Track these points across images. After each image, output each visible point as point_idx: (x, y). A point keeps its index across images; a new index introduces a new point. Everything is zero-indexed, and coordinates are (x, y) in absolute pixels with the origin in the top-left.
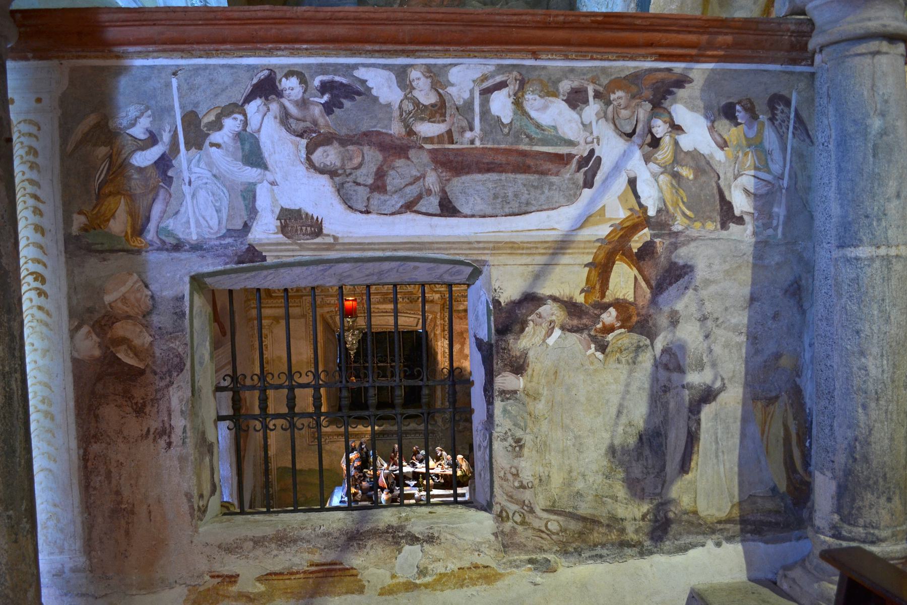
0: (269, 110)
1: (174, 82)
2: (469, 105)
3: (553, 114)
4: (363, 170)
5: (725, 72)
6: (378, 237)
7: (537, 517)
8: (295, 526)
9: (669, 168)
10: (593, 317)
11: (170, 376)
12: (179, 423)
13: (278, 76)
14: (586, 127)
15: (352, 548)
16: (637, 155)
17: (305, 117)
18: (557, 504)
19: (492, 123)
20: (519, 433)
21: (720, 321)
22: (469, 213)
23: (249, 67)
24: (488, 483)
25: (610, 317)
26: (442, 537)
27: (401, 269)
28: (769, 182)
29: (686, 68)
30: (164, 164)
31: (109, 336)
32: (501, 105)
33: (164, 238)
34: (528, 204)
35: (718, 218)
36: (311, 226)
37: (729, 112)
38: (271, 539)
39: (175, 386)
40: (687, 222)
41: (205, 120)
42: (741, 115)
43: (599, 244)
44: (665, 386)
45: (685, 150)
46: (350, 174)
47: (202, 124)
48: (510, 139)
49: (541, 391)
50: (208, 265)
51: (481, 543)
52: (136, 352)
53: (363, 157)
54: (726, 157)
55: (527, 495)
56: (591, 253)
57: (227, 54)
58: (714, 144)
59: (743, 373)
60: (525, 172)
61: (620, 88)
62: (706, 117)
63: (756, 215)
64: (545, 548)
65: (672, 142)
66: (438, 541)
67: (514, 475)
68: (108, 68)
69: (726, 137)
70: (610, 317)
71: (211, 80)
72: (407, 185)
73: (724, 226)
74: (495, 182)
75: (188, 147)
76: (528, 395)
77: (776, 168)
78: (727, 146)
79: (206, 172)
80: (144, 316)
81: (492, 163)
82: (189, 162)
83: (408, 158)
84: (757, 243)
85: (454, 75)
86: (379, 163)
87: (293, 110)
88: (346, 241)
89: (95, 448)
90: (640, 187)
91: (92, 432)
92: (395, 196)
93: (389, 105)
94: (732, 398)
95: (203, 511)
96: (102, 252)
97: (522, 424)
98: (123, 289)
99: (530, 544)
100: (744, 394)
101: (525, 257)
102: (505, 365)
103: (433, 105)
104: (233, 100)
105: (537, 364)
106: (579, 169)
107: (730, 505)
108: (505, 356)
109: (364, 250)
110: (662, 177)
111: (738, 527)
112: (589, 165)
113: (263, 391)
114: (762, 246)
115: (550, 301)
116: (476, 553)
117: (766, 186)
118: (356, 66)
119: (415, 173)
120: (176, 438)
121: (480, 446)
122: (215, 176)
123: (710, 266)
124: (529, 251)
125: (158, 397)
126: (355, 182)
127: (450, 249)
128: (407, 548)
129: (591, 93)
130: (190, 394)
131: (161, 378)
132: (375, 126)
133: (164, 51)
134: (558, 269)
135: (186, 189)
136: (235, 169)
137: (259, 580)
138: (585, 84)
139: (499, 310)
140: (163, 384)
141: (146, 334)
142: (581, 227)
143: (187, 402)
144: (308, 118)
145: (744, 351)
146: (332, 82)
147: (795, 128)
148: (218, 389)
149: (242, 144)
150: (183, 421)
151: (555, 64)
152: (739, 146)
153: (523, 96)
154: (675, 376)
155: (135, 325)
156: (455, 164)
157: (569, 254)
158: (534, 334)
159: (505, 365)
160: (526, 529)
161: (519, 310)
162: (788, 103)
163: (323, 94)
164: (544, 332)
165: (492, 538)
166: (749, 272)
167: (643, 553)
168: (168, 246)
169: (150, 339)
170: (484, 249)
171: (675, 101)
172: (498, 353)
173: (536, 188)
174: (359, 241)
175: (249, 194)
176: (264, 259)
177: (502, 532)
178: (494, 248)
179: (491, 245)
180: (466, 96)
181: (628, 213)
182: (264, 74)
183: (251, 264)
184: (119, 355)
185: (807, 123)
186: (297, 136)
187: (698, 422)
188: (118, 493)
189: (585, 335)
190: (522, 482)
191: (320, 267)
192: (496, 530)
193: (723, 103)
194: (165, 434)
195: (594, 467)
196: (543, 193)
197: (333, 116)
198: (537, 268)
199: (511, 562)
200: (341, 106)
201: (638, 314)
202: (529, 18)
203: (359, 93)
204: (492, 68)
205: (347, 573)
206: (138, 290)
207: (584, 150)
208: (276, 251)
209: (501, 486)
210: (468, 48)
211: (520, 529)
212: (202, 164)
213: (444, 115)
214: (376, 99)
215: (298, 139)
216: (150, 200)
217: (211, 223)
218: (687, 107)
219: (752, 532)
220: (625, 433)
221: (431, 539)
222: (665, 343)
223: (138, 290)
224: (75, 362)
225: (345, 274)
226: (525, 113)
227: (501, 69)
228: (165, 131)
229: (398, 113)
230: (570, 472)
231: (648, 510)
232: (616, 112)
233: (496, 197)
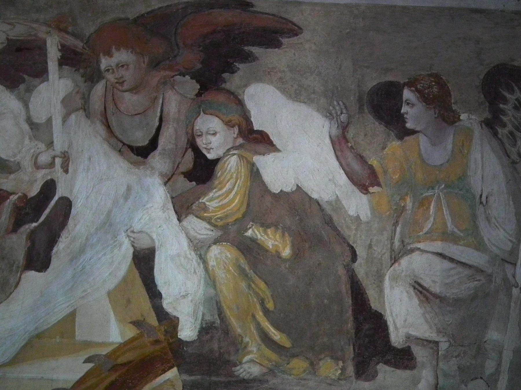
9: (233, 229)
14: (39, 130)
28: (479, 270)
35: (350, 351)
37: (384, 105)
40: (274, 356)
42: (413, 111)
45: (275, 188)
54: (373, 209)
58: (342, 178)
61: (121, 44)
62: (329, 116)
63: (444, 346)
65: (244, 171)
69: (374, 162)
73: (363, 369)
106: (17, 223)
110: (215, 251)
117: (471, 278)
129: (53, 54)
138: (42, 32)
181: (131, 332)
193: (371, 83)
207: (32, 182)
218: (284, 91)
232: (111, 97)
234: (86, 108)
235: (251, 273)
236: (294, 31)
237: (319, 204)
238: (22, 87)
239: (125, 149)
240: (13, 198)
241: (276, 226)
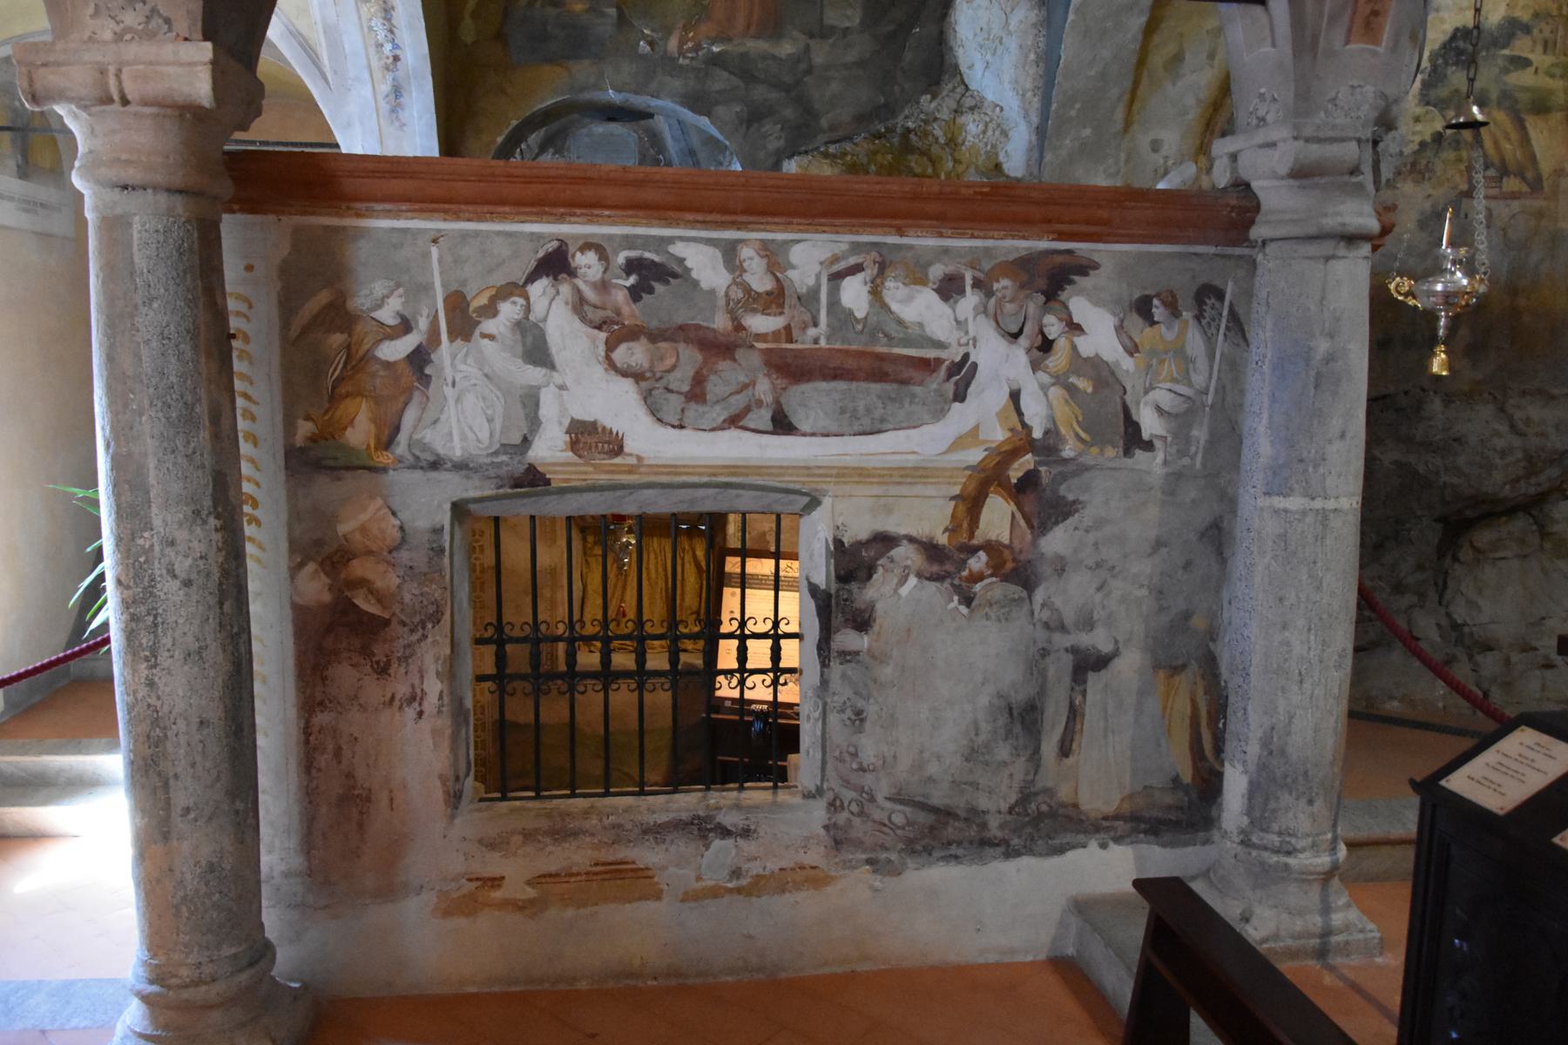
1: (434, 251)
2: (814, 292)
3: (919, 308)
4: (677, 374)
13: (571, 249)
14: (960, 324)
20: (860, 704)
23: (536, 238)
30: (419, 359)
31: (342, 576)
34: (883, 420)
36: (609, 443)
37: (1143, 308)
39: (430, 640)
41: (475, 304)
42: (1158, 312)
52: (380, 599)
55: (868, 780)
57: (504, 217)
58: (1121, 349)
61: (1006, 275)
62: (1114, 314)
65: (1068, 346)
68: (344, 228)
69: (1137, 340)
70: (978, 562)
71: (483, 252)
73: (1127, 452)
75: (453, 334)
76: (874, 657)
77: (1199, 379)
78: (1137, 350)
83: (735, 360)
85: (797, 254)
88: (652, 462)
89: (322, 718)
91: (319, 699)
92: (718, 408)
93: (712, 292)
94: (1130, 665)
96: (333, 469)
98: (363, 517)
103: (768, 293)
104: (512, 279)
106: (949, 376)
109: (677, 474)
112: (962, 375)
114: (1176, 479)
115: (905, 542)
118: (671, 240)
119: (743, 379)
122: (486, 376)
123: (1107, 503)
128: (717, 844)
129: (969, 281)
130: (448, 651)
131: (412, 631)
133: (422, 211)
135: (448, 391)
137: (528, 883)
147: (1227, 328)
148: (478, 641)
149: (523, 336)
151: (924, 242)
156: (793, 368)
162: (1220, 295)
163: (628, 274)
164: (895, 581)
165: (823, 832)
167: (1011, 853)
168: (424, 464)
169: (398, 581)
175: (531, 401)
176: (548, 482)
178: (838, 476)
179: (834, 472)
180: (811, 281)
181: (1008, 434)
182: (552, 246)
185: (1243, 319)
187: (1084, 694)
188: (350, 775)
189: (947, 584)
191: (618, 493)
193: (1137, 295)
197: (640, 304)
199: (844, 862)
200: (651, 291)
201: (1014, 560)
202: (895, 188)
203: (675, 276)
204: (845, 247)
205: (640, 874)
210: (817, 220)
211: (857, 821)
212: (470, 360)
213: (781, 306)
214: (696, 284)
216: (400, 405)
219: (1145, 832)
221: (746, 833)
224: (295, 607)
226: (885, 307)
233: (843, 411)
236: (1096, 266)
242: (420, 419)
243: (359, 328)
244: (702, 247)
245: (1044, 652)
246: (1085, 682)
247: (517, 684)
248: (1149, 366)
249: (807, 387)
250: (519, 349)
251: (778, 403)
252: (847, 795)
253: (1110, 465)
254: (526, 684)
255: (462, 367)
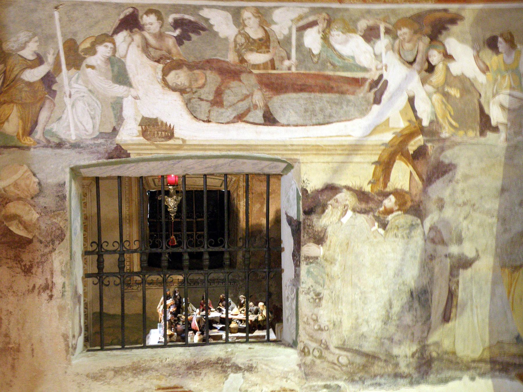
0: (133, 40)
1: (56, 14)
3: (353, 47)
4: (206, 89)
5: (491, 11)
6: (217, 140)
7: (331, 353)
8: (146, 358)
9: (440, 89)
10: (376, 202)
11: (53, 244)
12: (59, 280)
13: (140, 14)
14: (377, 57)
15: (190, 376)
16: (416, 78)
17: (161, 46)
18: (346, 343)
19: (305, 54)
20: (319, 289)
21: (477, 206)
22: (286, 123)
24: (295, 326)
25: (390, 202)
26: (259, 367)
27: (232, 164)
29: (459, 9)
30: (49, 80)
32: (312, 39)
33: (49, 138)
34: (330, 116)
35: (478, 128)
36: (165, 131)
37: (492, 44)
38: (128, 369)
39: (57, 251)
41: (83, 47)
42: (502, 45)
43: (383, 147)
44: (431, 255)
46: (196, 92)
47: (80, 50)
48: (318, 66)
49: (336, 257)
50: (84, 159)
51: (289, 372)
53: (206, 79)
54: (488, 80)
55: (324, 336)
56: (377, 154)
58: (477, 69)
59: (494, 247)
60: (329, 92)
61: (405, 26)
62: (473, 48)
63: (509, 125)
64: (337, 376)
65: (444, 68)
66: (256, 370)
67: (314, 320)
70: (390, 202)
71: (87, 14)
72: (239, 101)
73: (482, 133)
74: (306, 99)
75: (69, 66)
76: (326, 260)
79: (84, 87)
80: (32, 198)
81: (304, 85)
82: (70, 79)
83: (240, 81)
84: (508, 148)
86: (218, 84)
87: (152, 41)
88: (191, 143)
90: (418, 104)
92: (230, 110)
93: (226, 39)
94: (485, 266)
95: (74, 348)
97: (321, 282)
98: (15, 177)
99: (326, 374)
100: (495, 263)
101: (326, 156)
102: (310, 238)
103: (260, 40)
104: (104, 31)
105: (334, 237)
106: (371, 89)
107: (482, 349)
108: (310, 231)
109: (205, 150)
111: (489, 366)
112: (378, 87)
113: (122, 254)
116: (285, 380)
119: (245, 92)
120: (56, 292)
121: (288, 298)
122: (90, 91)
123: (470, 164)
124: (330, 153)
125: (43, 260)
126: (199, 98)
127: (271, 150)
128: (232, 376)
129: (382, 30)
130: (69, 258)
131: (46, 246)
132: (215, 55)
134: (351, 166)
135: (67, 100)
136: (106, 86)
138: (378, 22)
139: (307, 196)
140: (47, 250)
141: (34, 212)
142: (371, 134)
143: (67, 264)
144: (164, 48)
145: (495, 229)
146: (182, 19)
149: (112, 67)
150: (63, 279)
152: (499, 71)
153: (329, 32)
154: (440, 248)
155: (25, 205)
156: (275, 84)
157: (360, 154)
158: (332, 214)
159: (310, 238)
160: (322, 362)
161: (321, 196)
164: (339, 213)
165: (297, 368)
166: (501, 169)
168: (52, 144)
169: (37, 216)
170: (296, 150)
171: (449, 35)
172: (304, 228)
173: (337, 104)
174: (201, 143)
175: (117, 106)
176: (128, 155)
177: (304, 363)
178: (304, 150)
179: (301, 147)
180: (286, 32)
181: (407, 124)
183: (119, 160)
184: (11, 228)
186: (156, 61)
187: (457, 283)
188: (7, 335)
189: (371, 215)
190: (320, 326)
191: (171, 162)
192: (300, 362)
194: (48, 288)
195: (376, 316)
196: (342, 108)
197: (183, 47)
198: (335, 165)
199: (311, 387)
200: (189, 39)
203: (204, 29)
204: (306, 10)
206: (28, 178)
208: (138, 149)
209: (304, 329)
211: (318, 361)
212: (80, 81)
213: (268, 47)
214: (216, 34)
215: (156, 64)
216: (38, 109)
217: (87, 127)
218: (459, 40)
220: (400, 290)
221: (250, 369)
222: (432, 223)
223: (28, 178)
225: (189, 167)
226: (330, 46)
227: (314, 11)
228: (49, 54)
229: (233, 45)
230: (357, 318)
231: (417, 350)
232: (401, 45)
233: (306, 111)
234: (393, 49)
235: (446, 103)
237: (470, 80)
238: (372, 43)
239: (406, 63)
240: (369, 81)
241: (455, 87)
242: (50, 118)
243: (11, 61)
244: (220, 11)
245: (432, 258)
246: (458, 275)
247: (112, 279)
248: (496, 80)
249: (284, 97)
250: (110, 75)
251: (266, 106)
252: (313, 345)
253: (473, 141)
254: (115, 278)
255: (76, 86)
